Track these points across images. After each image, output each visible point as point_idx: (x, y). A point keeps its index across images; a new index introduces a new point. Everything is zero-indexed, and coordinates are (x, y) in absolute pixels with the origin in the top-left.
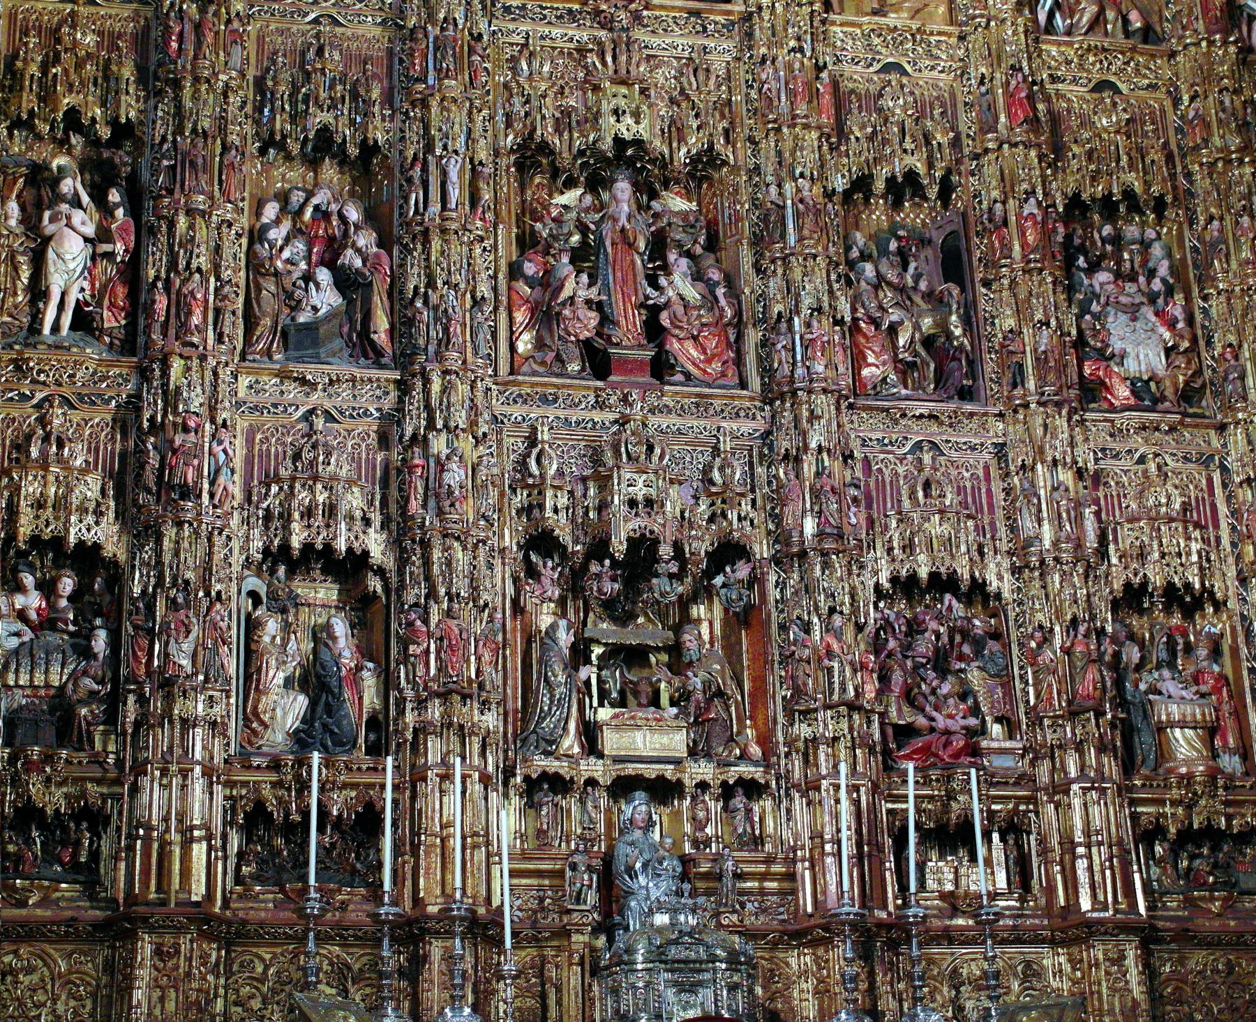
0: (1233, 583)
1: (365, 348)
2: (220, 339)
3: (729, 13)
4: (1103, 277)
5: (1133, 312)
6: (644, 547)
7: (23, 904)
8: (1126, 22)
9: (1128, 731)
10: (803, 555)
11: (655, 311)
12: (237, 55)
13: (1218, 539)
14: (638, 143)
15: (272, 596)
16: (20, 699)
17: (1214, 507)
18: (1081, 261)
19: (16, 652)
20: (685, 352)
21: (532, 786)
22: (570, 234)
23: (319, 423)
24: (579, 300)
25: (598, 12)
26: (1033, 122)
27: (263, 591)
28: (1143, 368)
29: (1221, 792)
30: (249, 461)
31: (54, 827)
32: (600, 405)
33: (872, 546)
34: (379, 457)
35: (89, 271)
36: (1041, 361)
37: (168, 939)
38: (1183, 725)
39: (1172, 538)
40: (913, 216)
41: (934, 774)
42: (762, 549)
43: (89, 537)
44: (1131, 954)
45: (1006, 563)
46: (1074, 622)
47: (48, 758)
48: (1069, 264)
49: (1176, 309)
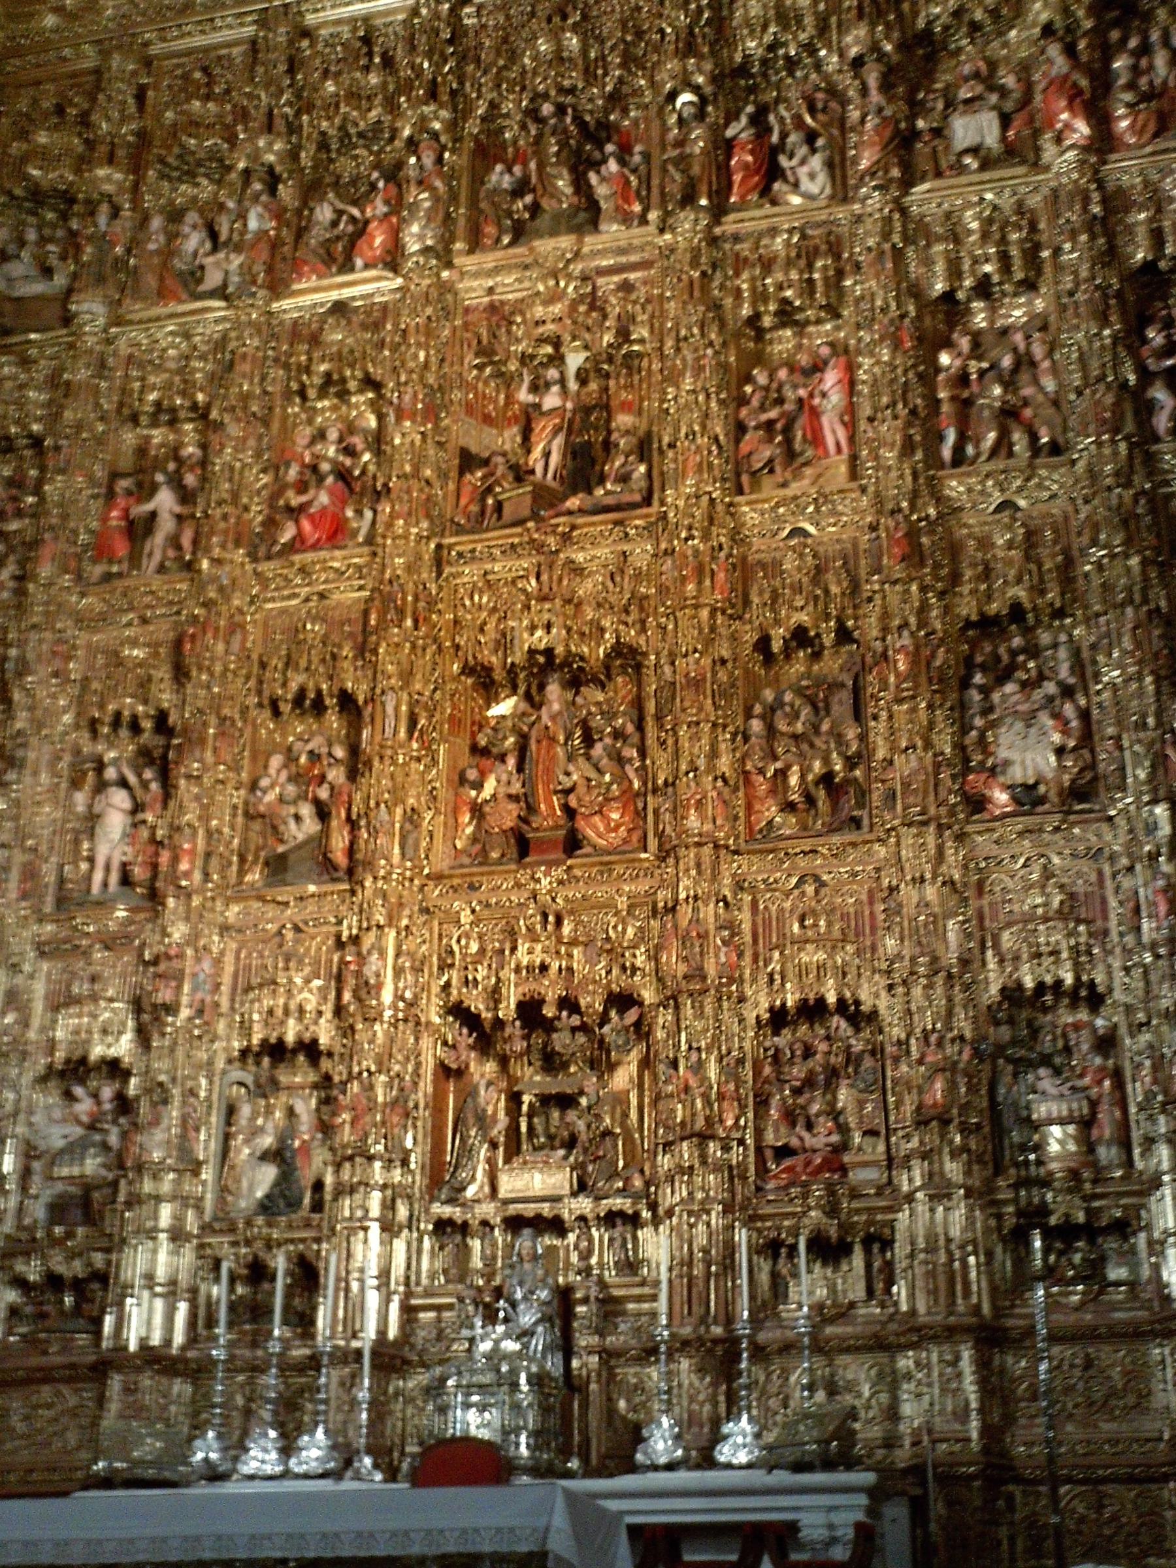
0: (1119, 975)
1: (327, 866)
2: (206, 876)
3: (647, 516)
4: (1009, 688)
5: (1030, 718)
6: (529, 1010)
7: (45, 1353)
8: (1034, 437)
9: (998, 1132)
10: (674, 998)
11: (568, 792)
12: (237, 639)
13: (1106, 933)
14: (549, 652)
15: (258, 1085)
16: (60, 1187)
17: (1104, 901)
18: (978, 679)
19: (62, 1152)
20: (592, 830)
21: (442, 1226)
22: (505, 738)
23: (289, 935)
24: (500, 796)
25: (532, 541)
26: (914, 556)
27: (249, 1080)
28: (1030, 772)
29: (1087, 1186)
30: (236, 976)
31: (78, 1286)
32: (518, 885)
33: (754, 980)
34: (336, 958)
35: (129, 836)
36: (906, 785)
37: (132, 1377)
38: (1051, 1122)
39: (1053, 936)
40: (832, 665)
41: (794, 1191)
42: (648, 996)
43: (113, 1052)
44: (966, 1354)
45: (884, 982)
46: (926, 1034)
47: (70, 1235)
48: (965, 684)
49: (1069, 709)
